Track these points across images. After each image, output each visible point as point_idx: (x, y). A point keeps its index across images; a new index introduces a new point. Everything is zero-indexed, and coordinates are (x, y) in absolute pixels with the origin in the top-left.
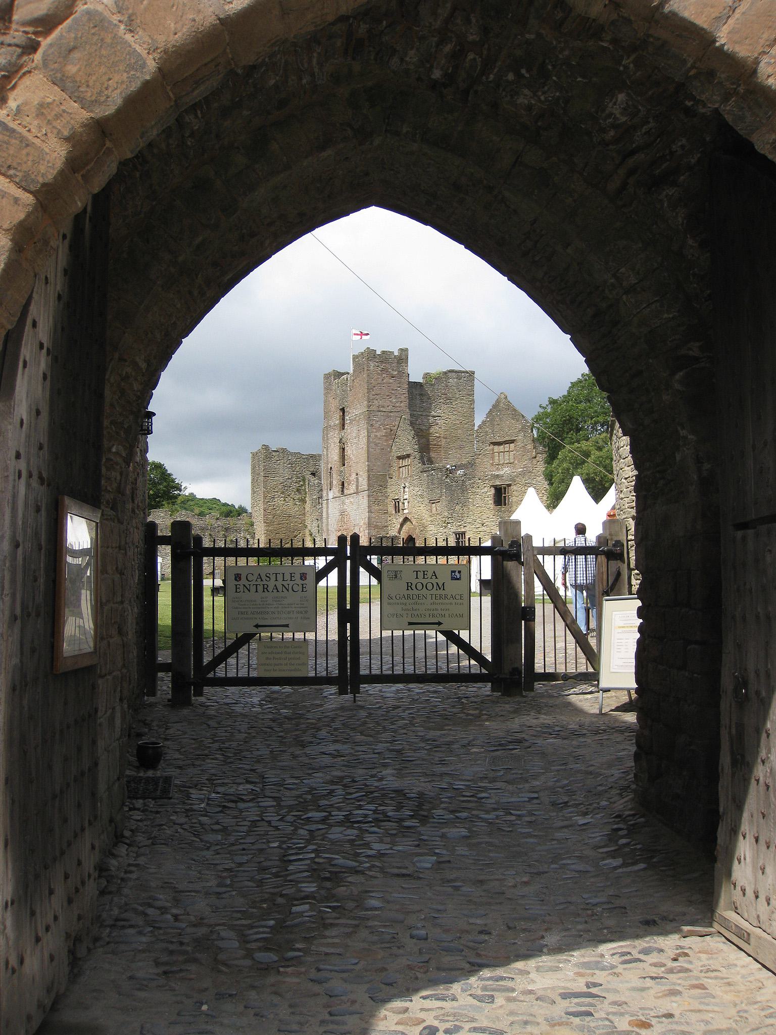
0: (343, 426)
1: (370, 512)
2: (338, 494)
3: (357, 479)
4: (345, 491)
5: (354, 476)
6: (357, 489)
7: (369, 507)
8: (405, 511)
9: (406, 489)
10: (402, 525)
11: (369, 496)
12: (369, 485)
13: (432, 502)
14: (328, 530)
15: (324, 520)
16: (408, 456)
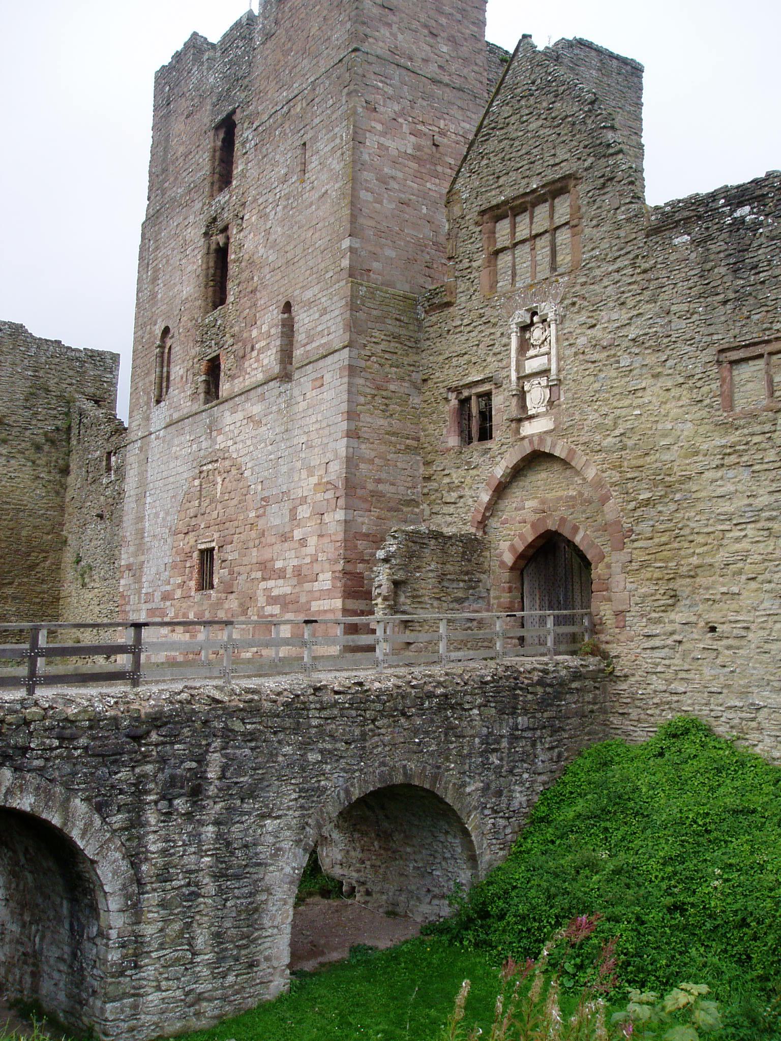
0: (223, 175)
1: (352, 434)
2: (199, 405)
3: (288, 328)
4: (225, 388)
5: (269, 320)
6: (286, 355)
7: (351, 415)
8: (528, 429)
9: (537, 334)
10: (501, 490)
11: (352, 370)
12: (354, 327)
13: (730, 358)
14: (140, 533)
15: (129, 505)
16: (557, 189)
